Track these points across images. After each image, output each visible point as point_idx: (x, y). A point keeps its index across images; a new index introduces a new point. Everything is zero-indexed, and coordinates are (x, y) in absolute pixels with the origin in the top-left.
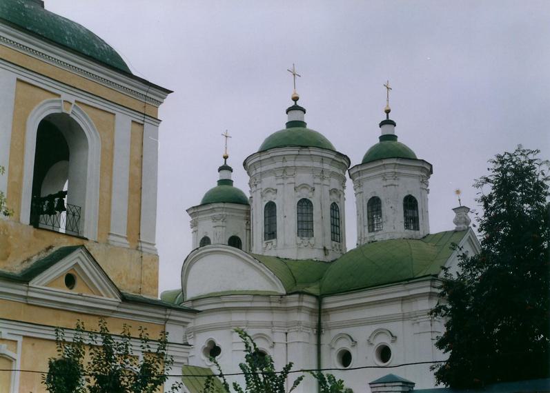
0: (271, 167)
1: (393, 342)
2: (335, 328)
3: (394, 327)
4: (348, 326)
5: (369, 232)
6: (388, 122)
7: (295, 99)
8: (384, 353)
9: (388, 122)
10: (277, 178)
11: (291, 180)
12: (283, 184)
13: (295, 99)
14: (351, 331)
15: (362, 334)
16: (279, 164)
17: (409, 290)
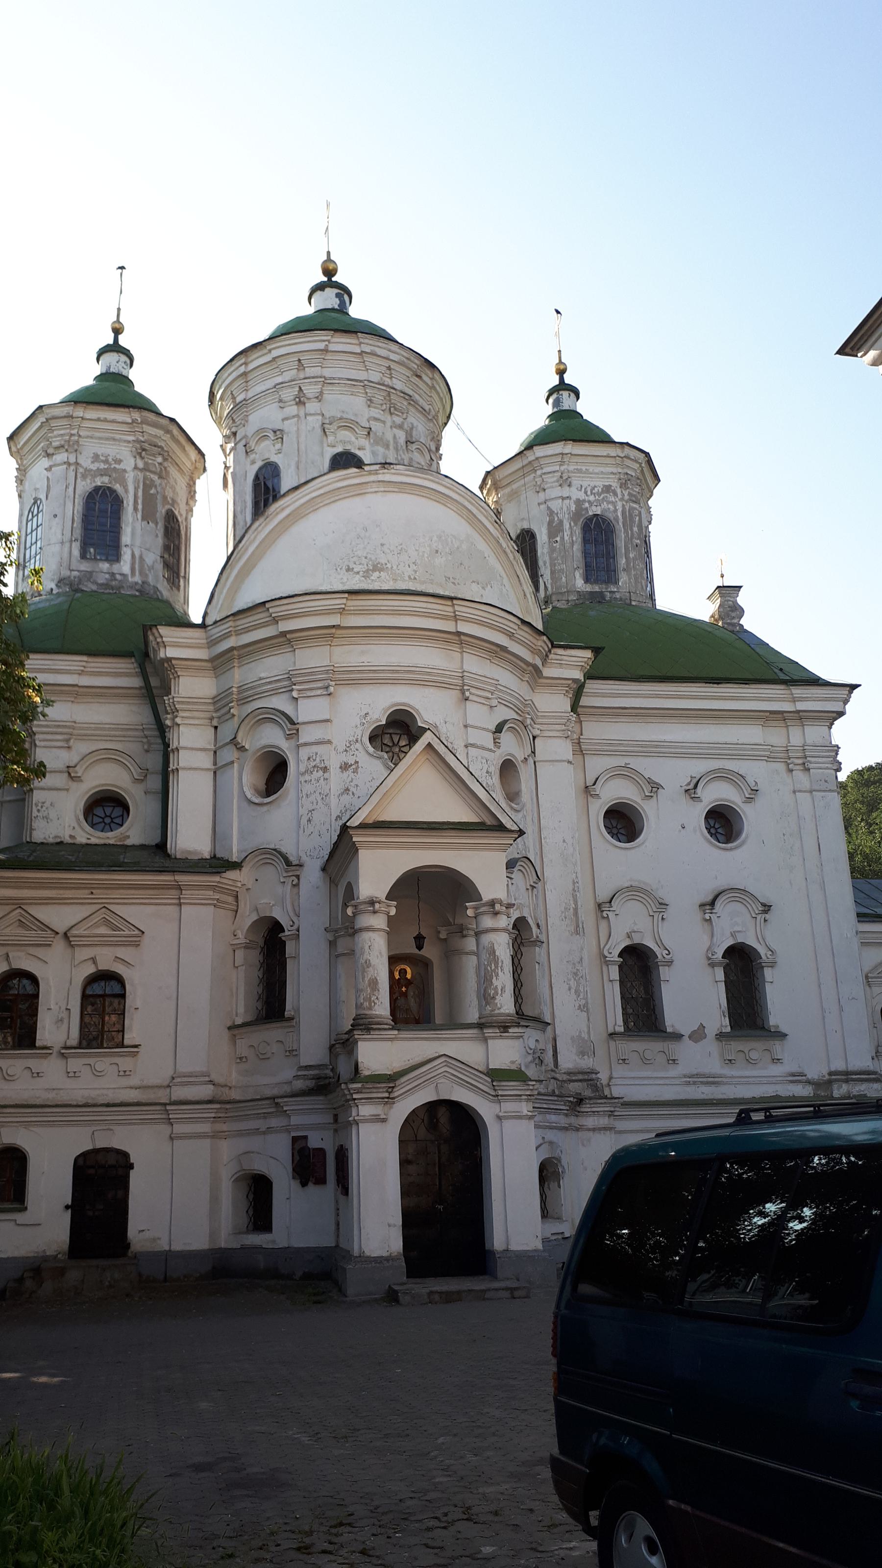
0: (362, 375)
1: (749, 800)
2: (597, 753)
3: (755, 771)
4: (647, 754)
5: (587, 580)
6: (562, 387)
7: (329, 270)
8: (723, 824)
9: (562, 387)
10: (370, 402)
11: (398, 420)
12: (384, 422)
14: (649, 767)
15: (673, 774)
16: (375, 377)
17: (794, 700)
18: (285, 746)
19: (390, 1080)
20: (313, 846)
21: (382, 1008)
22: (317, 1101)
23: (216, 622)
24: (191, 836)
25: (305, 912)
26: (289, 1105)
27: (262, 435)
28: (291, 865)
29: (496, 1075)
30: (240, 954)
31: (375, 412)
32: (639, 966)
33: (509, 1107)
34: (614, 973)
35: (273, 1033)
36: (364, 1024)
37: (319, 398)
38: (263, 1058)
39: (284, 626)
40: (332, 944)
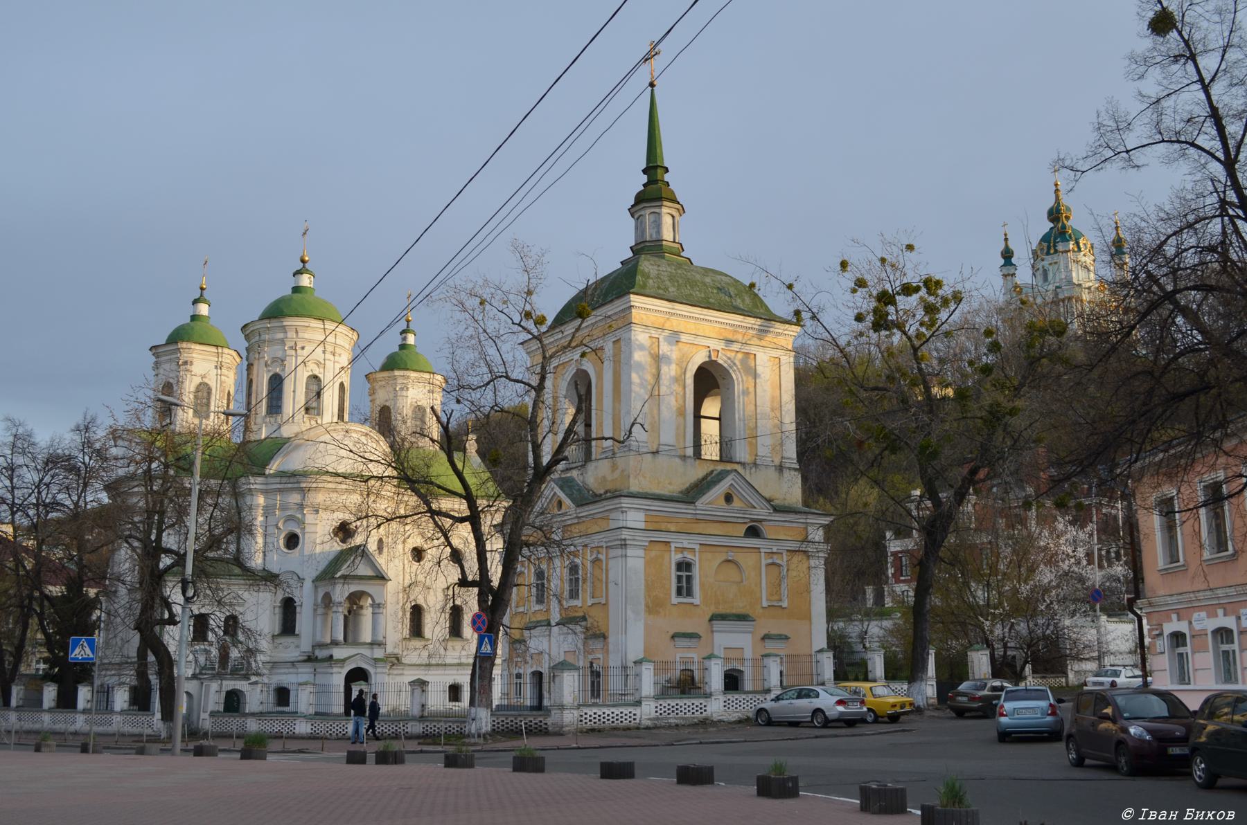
13: (303, 261)
18: (298, 531)
19: (344, 661)
20: (310, 573)
21: (341, 638)
22: (309, 664)
23: (270, 475)
24: (257, 562)
25: (305, 598)
26: (298, 665)
27: (274, 360)
28: (301, 580)
29: (376, 660)
30: (277, 610)
31: (328, 356)
32: (417, 612)
33: (379, 670)
34: (408, 615)
35: (288, 640)
36: (335, 643)
37: (303, 348)
38: (286, 648)
39: (303, 485)
40: (315, 610)
